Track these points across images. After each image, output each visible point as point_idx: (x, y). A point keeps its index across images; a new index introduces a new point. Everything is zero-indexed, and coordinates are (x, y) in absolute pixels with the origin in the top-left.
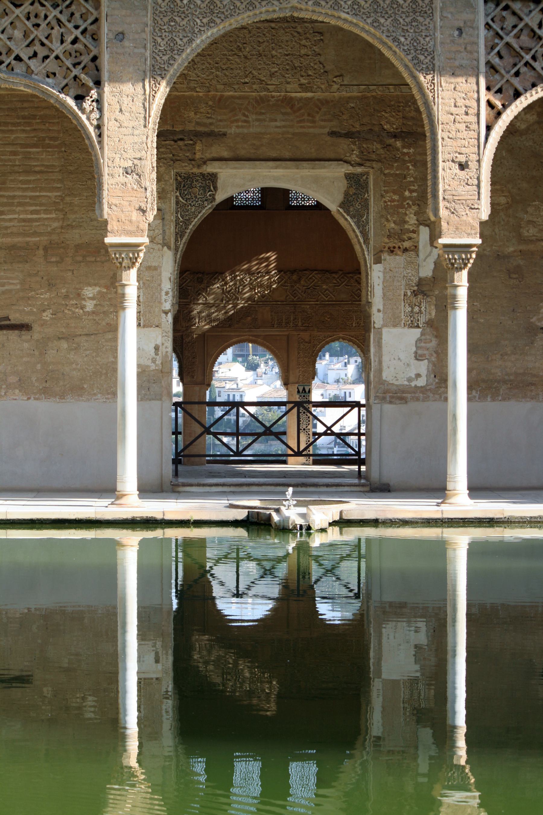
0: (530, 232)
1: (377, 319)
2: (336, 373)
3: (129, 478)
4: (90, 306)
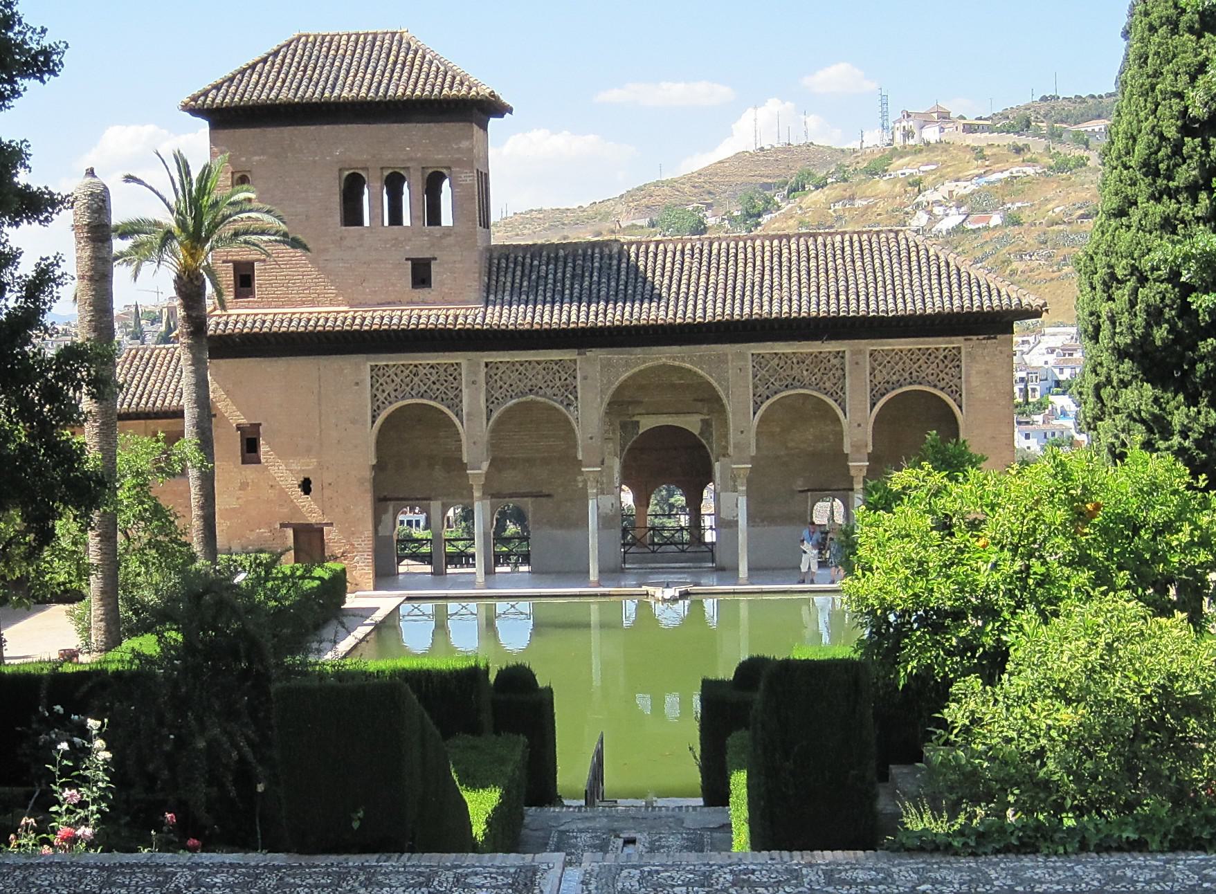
0: (791, 444)
3: (594, 575)
4: (580, 485)
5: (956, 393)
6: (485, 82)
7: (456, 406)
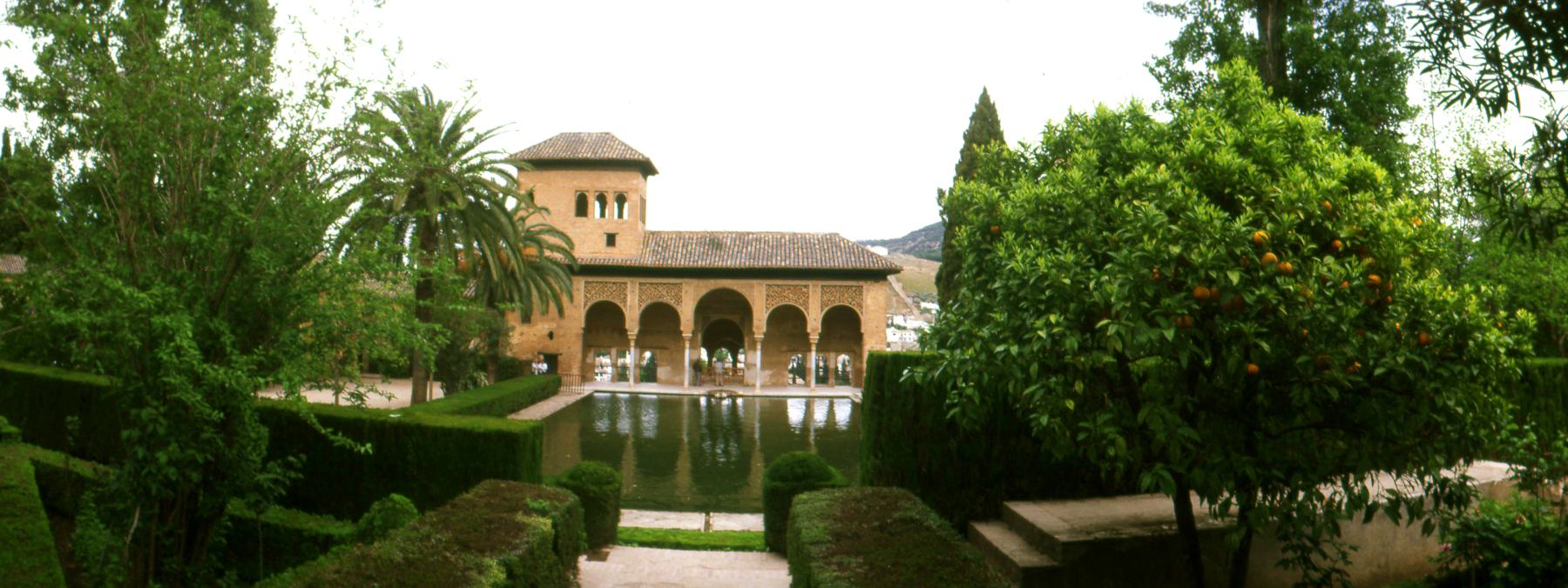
5: (860, 306)
6: (643, 147)
7: (624, 300)
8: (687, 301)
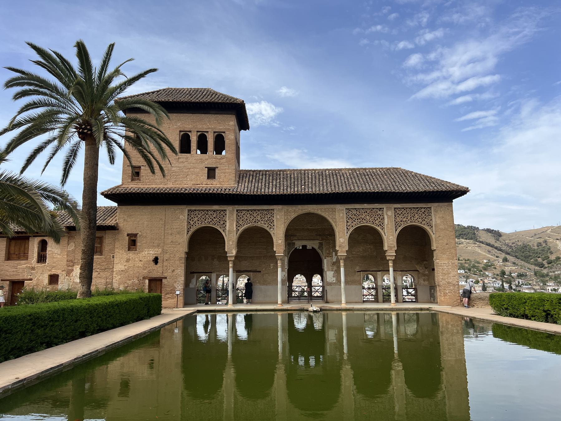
1: (326, 269)
2: (316, 280)
4: (272, 267)
8: (278, 223)
